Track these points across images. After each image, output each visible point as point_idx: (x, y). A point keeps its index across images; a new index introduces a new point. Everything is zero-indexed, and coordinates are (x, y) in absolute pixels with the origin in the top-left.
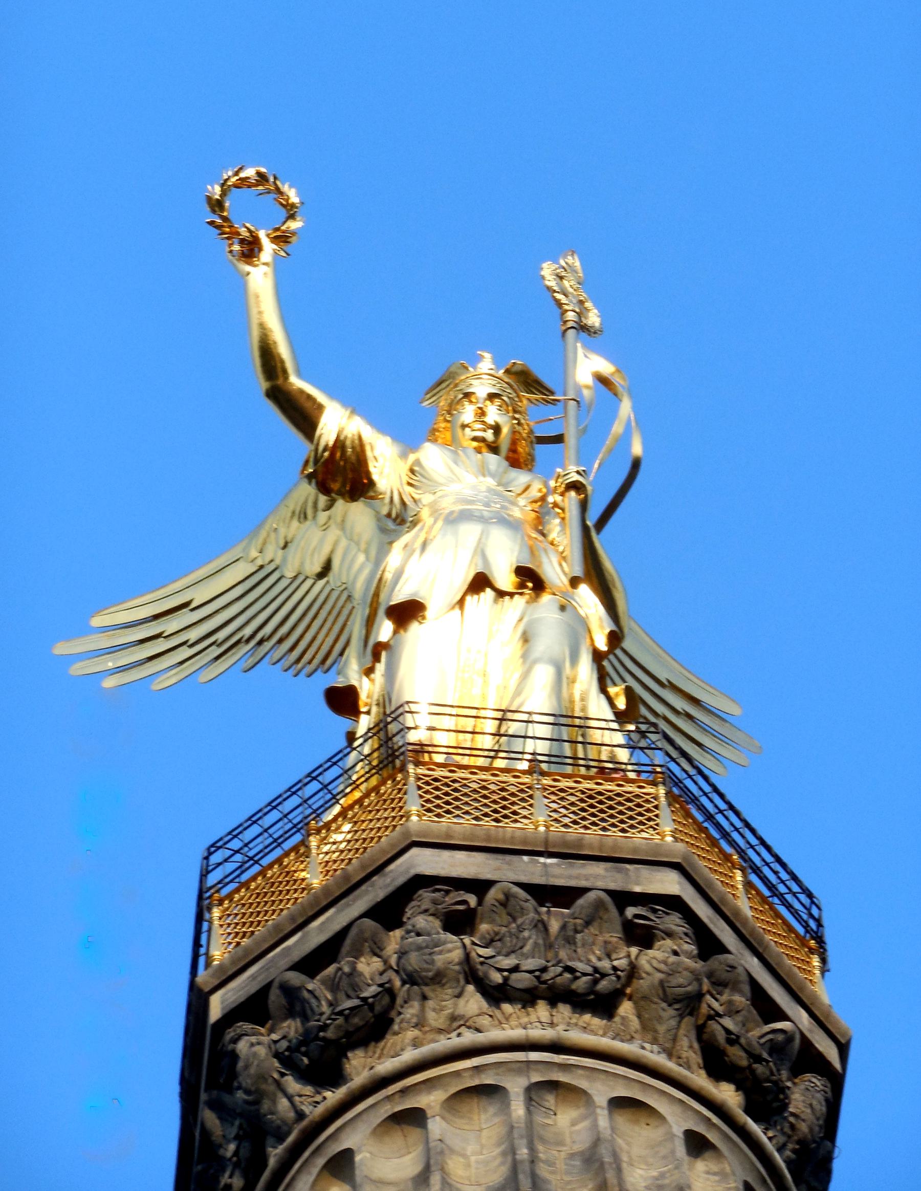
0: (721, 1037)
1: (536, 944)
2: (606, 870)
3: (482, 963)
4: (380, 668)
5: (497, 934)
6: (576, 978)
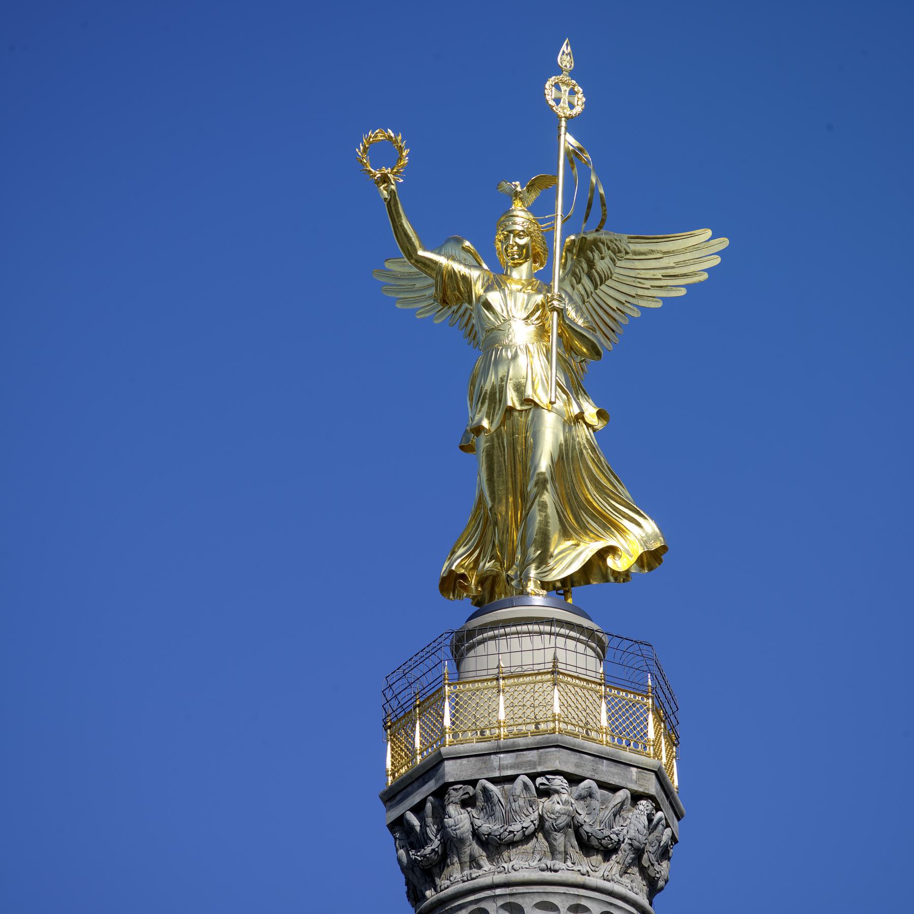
0: (585, 837)
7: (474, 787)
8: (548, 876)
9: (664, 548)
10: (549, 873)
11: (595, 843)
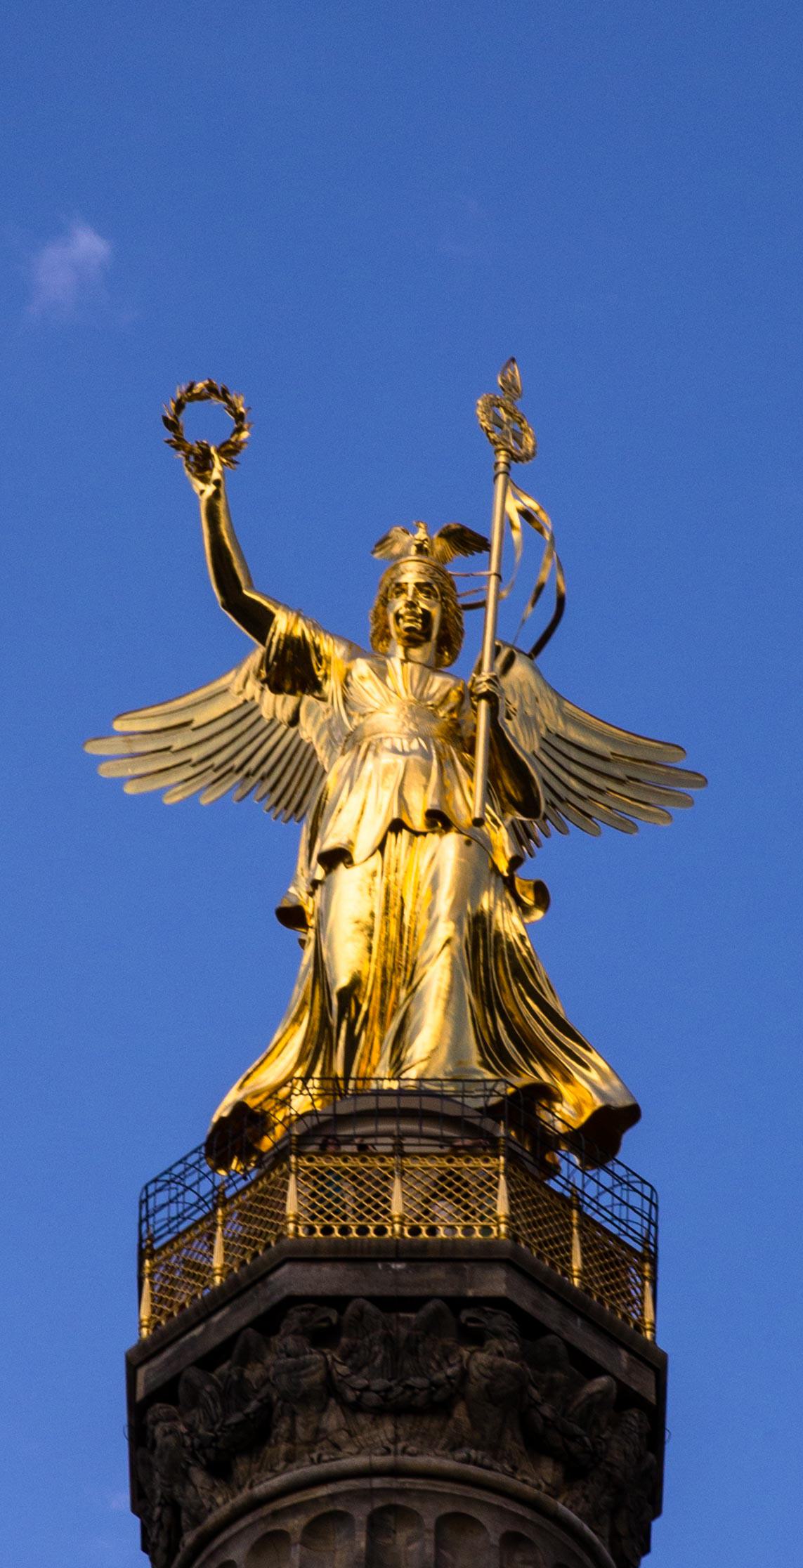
1: (384, 1358)
3: (340, 1381)
4: (318, 893)
6: (415, 1395)
7: (341, 1312)
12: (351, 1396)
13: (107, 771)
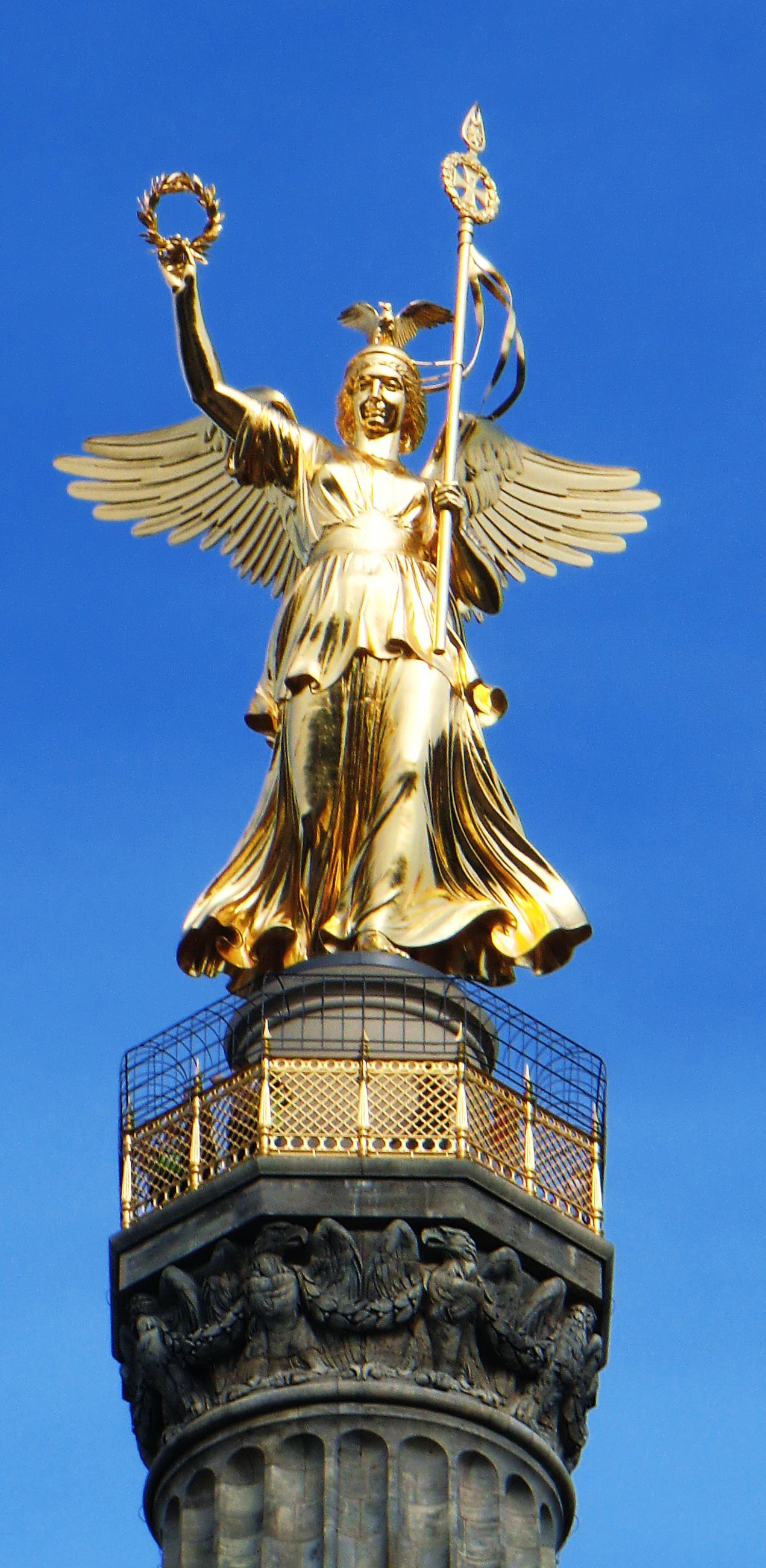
0: (494, 1341)
2: (409, 1190)
3: (310, 1301)
5: (323, 1264)
8: (432, 1394)
9: (584, 933)
10: (434, 1391)
11: (509, 1354)
12: (321, 1317)
13: (75, 491)
